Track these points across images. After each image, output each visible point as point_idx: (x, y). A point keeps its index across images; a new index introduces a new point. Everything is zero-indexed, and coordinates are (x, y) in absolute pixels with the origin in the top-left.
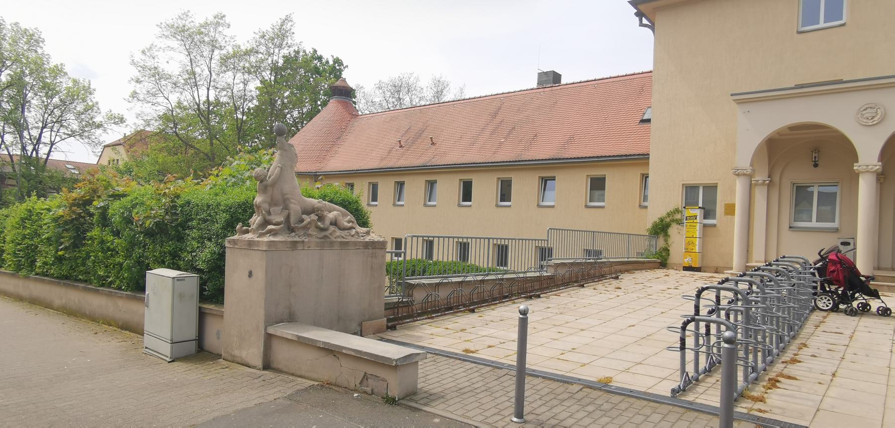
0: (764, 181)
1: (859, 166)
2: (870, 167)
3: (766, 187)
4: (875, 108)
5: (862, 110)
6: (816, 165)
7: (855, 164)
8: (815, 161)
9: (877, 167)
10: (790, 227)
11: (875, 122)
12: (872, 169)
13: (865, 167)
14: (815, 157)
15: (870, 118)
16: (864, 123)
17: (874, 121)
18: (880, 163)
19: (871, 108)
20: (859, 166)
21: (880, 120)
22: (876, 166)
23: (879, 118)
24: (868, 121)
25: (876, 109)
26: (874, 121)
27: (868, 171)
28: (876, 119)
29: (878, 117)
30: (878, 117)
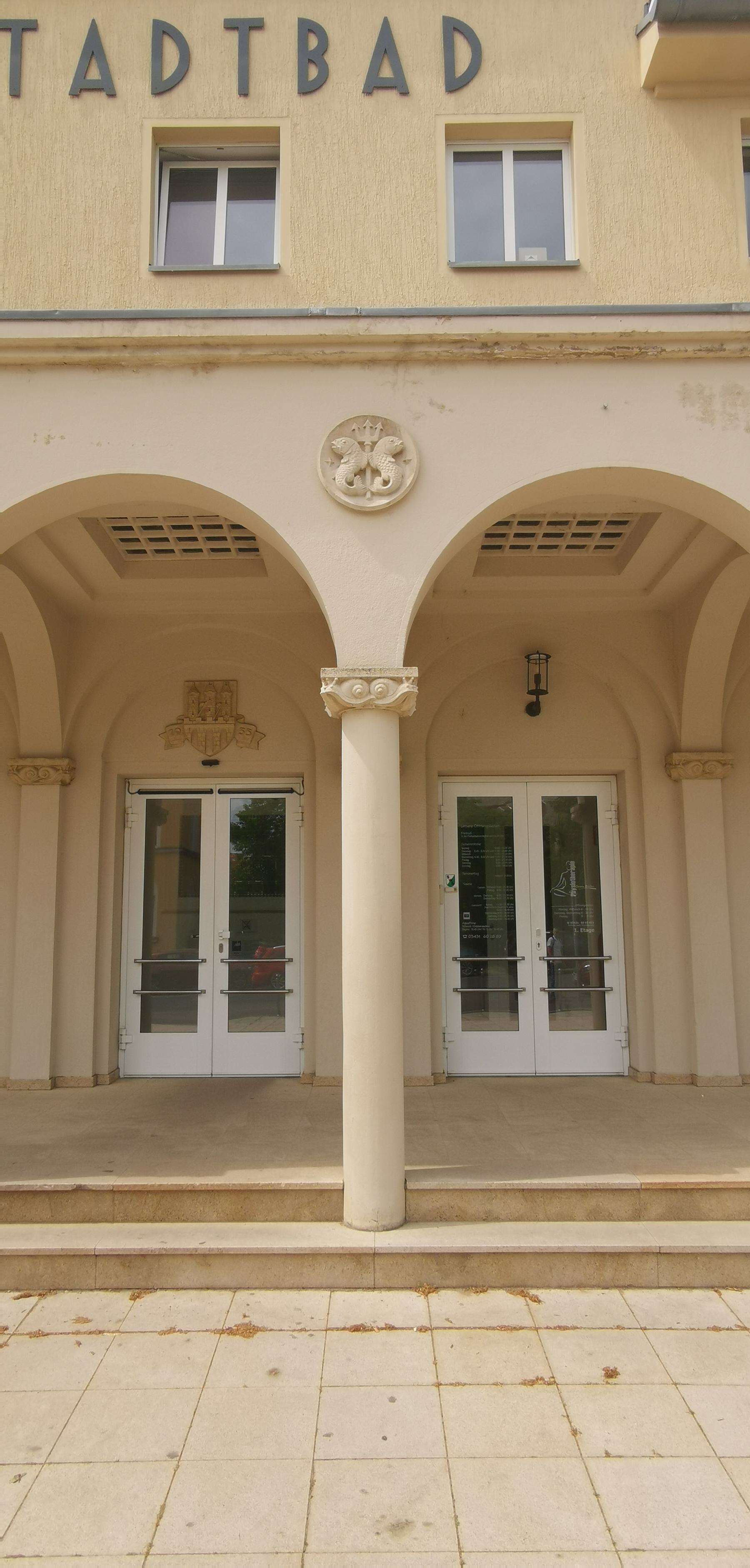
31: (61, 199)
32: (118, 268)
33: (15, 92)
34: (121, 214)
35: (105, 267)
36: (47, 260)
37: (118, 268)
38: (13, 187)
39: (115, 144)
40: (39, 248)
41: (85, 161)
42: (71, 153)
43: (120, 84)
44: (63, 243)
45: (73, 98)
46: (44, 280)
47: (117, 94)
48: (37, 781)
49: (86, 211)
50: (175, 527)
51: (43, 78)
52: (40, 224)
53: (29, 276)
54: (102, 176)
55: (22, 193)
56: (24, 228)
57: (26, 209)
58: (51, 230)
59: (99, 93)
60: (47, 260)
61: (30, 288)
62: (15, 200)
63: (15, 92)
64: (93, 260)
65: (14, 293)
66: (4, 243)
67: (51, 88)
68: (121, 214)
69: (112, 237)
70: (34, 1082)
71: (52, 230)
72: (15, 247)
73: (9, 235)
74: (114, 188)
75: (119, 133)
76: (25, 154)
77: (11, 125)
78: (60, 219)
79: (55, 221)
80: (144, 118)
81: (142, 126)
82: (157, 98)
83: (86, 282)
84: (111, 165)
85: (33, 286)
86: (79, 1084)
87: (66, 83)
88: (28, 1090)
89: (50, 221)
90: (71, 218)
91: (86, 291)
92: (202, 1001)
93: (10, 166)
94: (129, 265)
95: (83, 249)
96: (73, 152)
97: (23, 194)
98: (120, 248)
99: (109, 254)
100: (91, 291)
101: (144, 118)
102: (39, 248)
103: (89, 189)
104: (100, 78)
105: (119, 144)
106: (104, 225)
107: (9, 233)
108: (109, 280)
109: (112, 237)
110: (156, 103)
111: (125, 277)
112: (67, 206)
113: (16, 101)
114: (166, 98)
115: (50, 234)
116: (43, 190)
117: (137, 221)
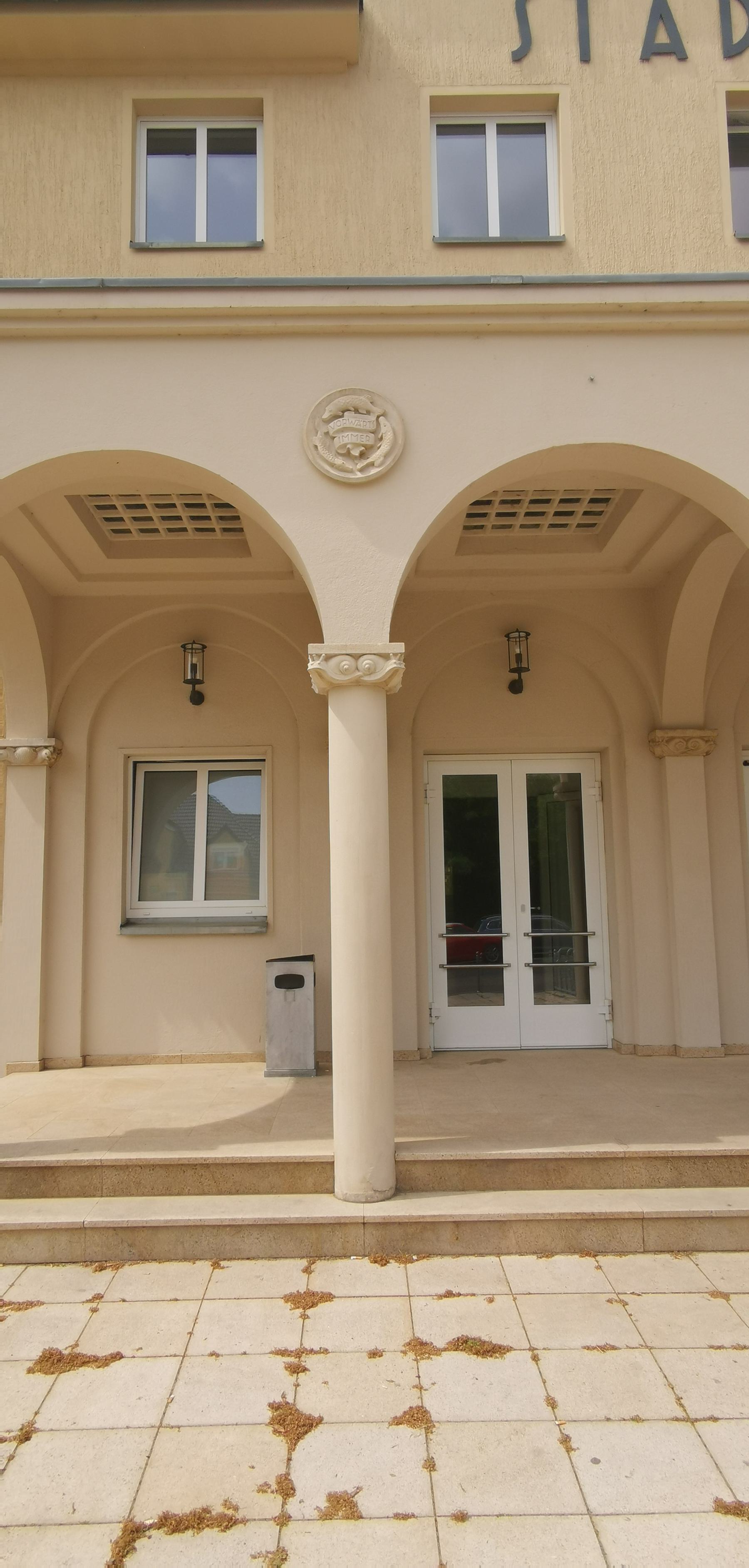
0: (35, 749)
1: (328, 658)
2: (365, 662)
3: (41, 775)
4: (368, 412)
5: (326, 416)
6: (197, 698)
7: (312, 648)
8: (194, 682)
9: (392, 664)
10: (127, 923)
11: (373, 471)
12: (371, 671)
13: (346, 663)
14: (194, 667)
15: (356, 453)
16: (334, 472)
17: (372, 464)
18: (400, 647)
19: (356, 411)
20: (328, 658)
21: (389, 461)
22: (386, 657)
23: (386, 456)
24: (349, 465)
25: (373, 418)
26: (372, 464)
27: (358, 683)
28: (376, 456)
29: (385, 447)
30: (385, 447)
31: (639, 166)
32: (701, 236)
33: (585, 57)
34: (701, 180)
35: (689, 235)
36: (630, 229)
37: (701, 236)
38: (589, 154)
39: (689, 109)
40: (620, 217)
41: (660, 127)
42: (645, 118)
43: (690, 47)
44: (644, 211)
45: (643, 62)
46: (628, 249)
47: (688, 56)
48: (685, 752)
49: (665, 178)
50: (188, 505)
51: (610, 43)
52: (619, 192)
53: (613, 245)
54: (679, 142)
55: (599, 160)
56: (604, 196)
57: (604, 176)
58: (631, 197)
59: (669, 57)
60: (630, 229)
61: (615, 257)
62: (592, 168)
63: (585, 57)
64: (676, 228)
65: (599, 262)
66: (585, 211)
67: (619, 53)
68: (701, 180)
69: (693, 204)
70: (708, 1050)
71: (632, 197)
72: (596, 216)
73: (589, 204)
74: (691, 154)
75: (693, 98)
76: (599, 121)
77: (583, 91)
78: (640, 187)
79: (634, 188)
80: (716, 82)
81: (715, 90)
82: (728, 61)
83: (670, 251)
84: (687, 129)
85: (618, 256)
86: (743, 1051)
87: (637, 47)
88: (703, 1057)
89: (630, 189)
90: (650, 186)
91: (672, 259)
92: (507, 975)
93: (585, 133)
94: (713, 232)
95: (665, 217)
96: (647, 118)
97: (600, 162)
98: (702, 215)
99: (692, 221)
100: (676, 260)
101: (716, 82)
102: (620, 217)
103: (666, 155)
104: (668, 42)
105: (693, 109)
106: (684, 191)
107: (589, 201)
108: (694, 248)
109: (693, 204)
110: (727, 67)
111: (710, 245)
112: (645, 173)
113: (586, 67)
114: (737, 61)
115: (631, 202)
116: (620, 157)
117: (718, 186)
